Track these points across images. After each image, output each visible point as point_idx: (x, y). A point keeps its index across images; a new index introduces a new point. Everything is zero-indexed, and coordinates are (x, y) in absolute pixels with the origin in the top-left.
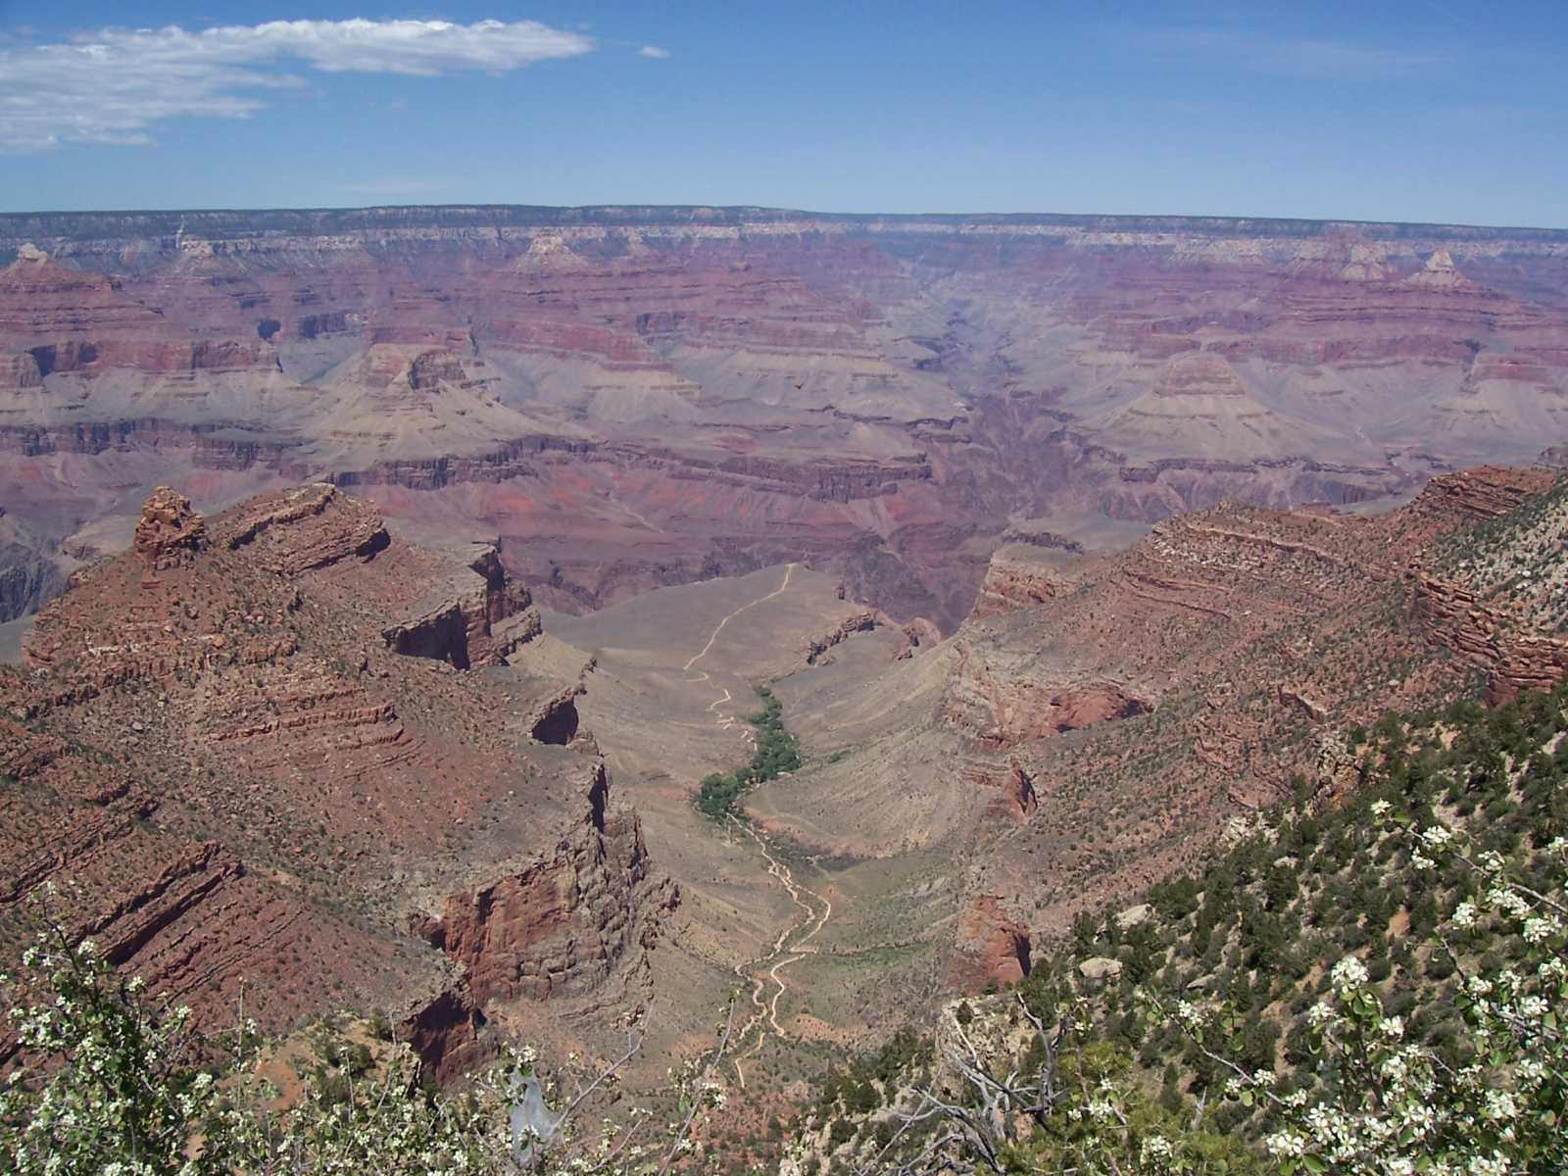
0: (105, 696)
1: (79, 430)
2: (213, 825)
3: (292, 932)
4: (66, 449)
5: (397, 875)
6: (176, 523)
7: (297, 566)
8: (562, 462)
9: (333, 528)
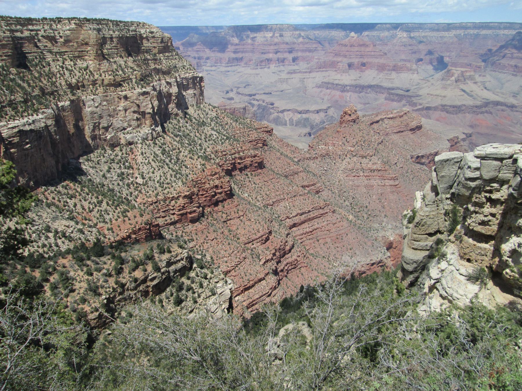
0: (319, 159)
1: (356, 86)
2: (337, 199)
3: (343, 231)
4: (351, 91)
5: (384, 224)
6: (350, 115)
7: (390, 132)
8: (503, 110)
9: (404, 122)
